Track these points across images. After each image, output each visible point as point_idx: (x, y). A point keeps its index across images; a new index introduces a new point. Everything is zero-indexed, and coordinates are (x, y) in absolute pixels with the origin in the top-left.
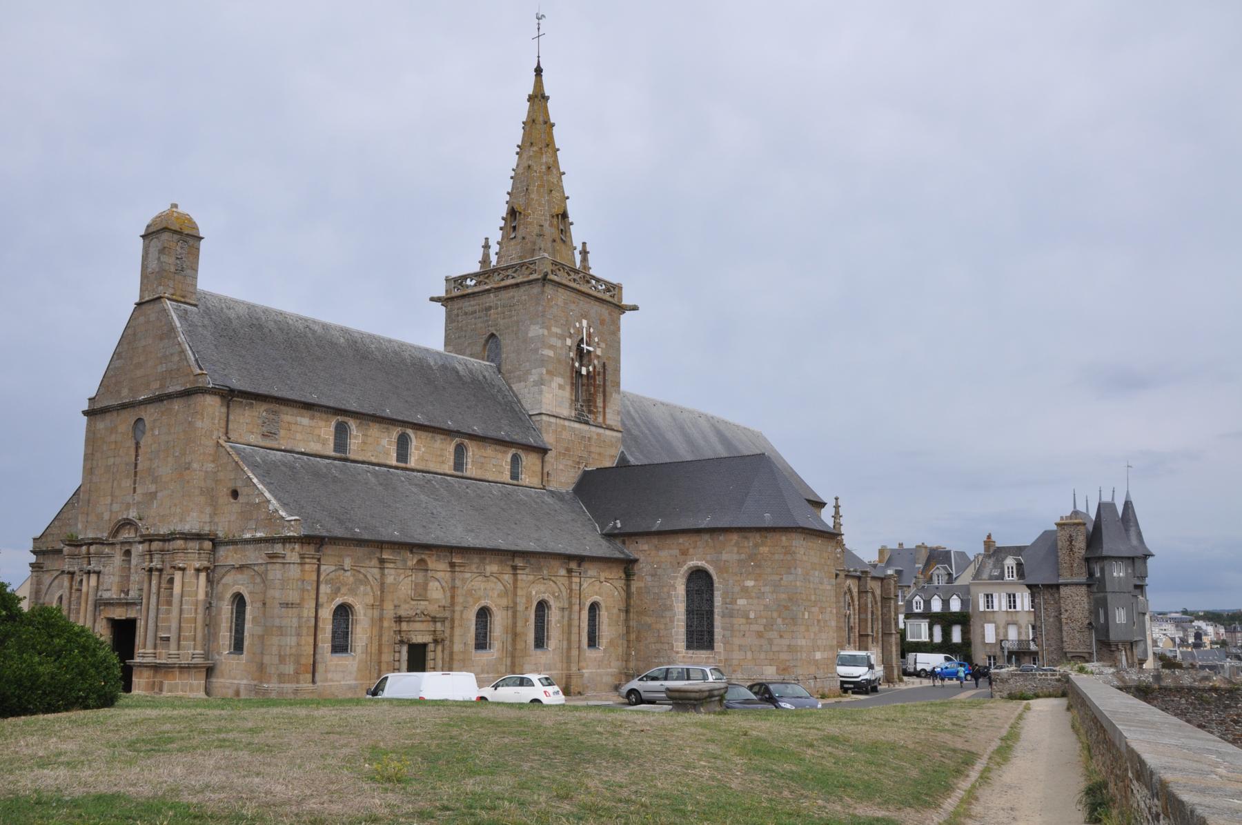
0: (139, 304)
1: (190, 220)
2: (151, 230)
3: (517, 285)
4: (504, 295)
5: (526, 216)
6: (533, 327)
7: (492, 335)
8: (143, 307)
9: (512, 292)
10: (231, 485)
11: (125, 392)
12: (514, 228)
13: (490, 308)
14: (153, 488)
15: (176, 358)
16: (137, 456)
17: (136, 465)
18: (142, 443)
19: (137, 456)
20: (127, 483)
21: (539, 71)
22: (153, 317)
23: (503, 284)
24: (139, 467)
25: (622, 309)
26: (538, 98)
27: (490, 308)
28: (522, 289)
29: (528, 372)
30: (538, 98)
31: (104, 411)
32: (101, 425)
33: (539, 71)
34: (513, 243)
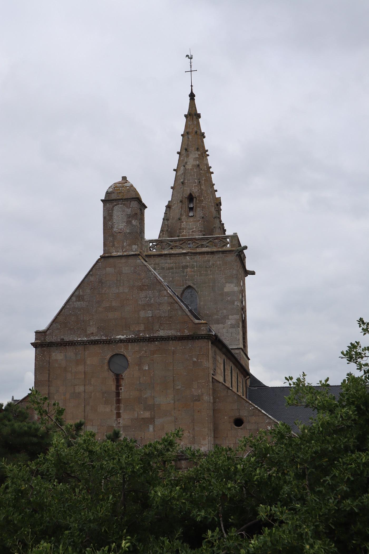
0: (102, 257)
1: (135, 190)
2: (113, 197)
3: (212, 253)
4: (198, 258)
5: (201, 201)
6: (228, 285)
7: (189, 287)
8: (111, 260)
9: (207, 257)
10: (236, 415)
11: (92, 329)
12: (191, 209)
13: (186, 267)
14: (147, 415)
15: (166, 308)
16: (118, 386)
17: (118, 394)
18: (125, 374)
19: (118, 386)
20: (110, 409)
21: (192, 96)
22: (126, 270)
23: (198, 250)
24: (122, 396)
25: (247, 273)
26: (193, 116)
27: (186, 267)
28: (217, 256)
29: (226, 317)
30: (193, 116)
31: (63, 344)
32: (58, 356)
33: (192, 96)
34: (192, 219)
